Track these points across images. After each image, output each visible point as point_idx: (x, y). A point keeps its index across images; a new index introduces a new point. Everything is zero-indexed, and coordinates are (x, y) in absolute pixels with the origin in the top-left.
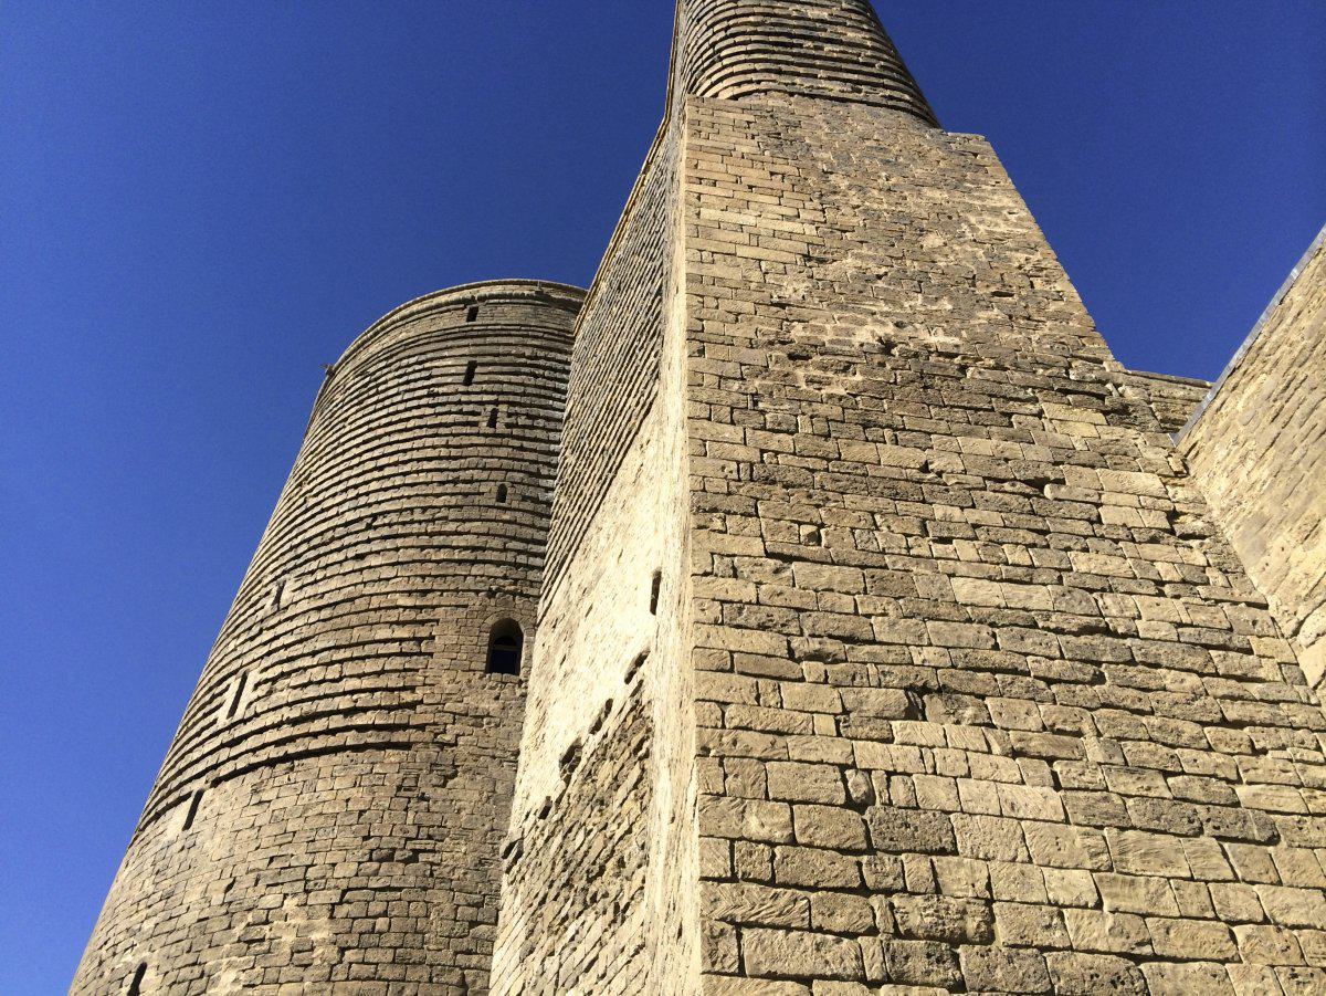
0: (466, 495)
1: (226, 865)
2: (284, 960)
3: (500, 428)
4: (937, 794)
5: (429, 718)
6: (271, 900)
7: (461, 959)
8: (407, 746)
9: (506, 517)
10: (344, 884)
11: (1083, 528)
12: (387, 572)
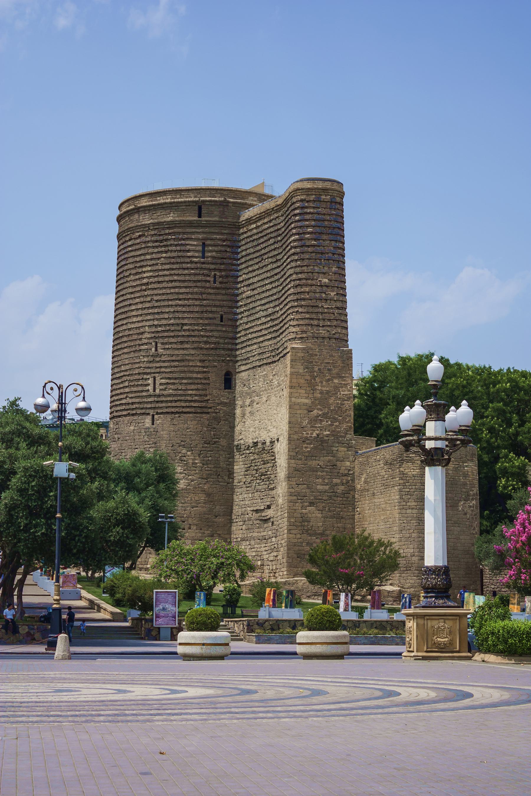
0: (210, 319)
1: (170, 440)
2: (191, 466)
3: (217, 285)
4: (310, 515)
5: (212, 405)
6: (184, 451)
7: (228, 467)
8: (208, 413)
9: (224, 329)
10: (200, 449)
11: (336, 474)
12: (193, 352)
